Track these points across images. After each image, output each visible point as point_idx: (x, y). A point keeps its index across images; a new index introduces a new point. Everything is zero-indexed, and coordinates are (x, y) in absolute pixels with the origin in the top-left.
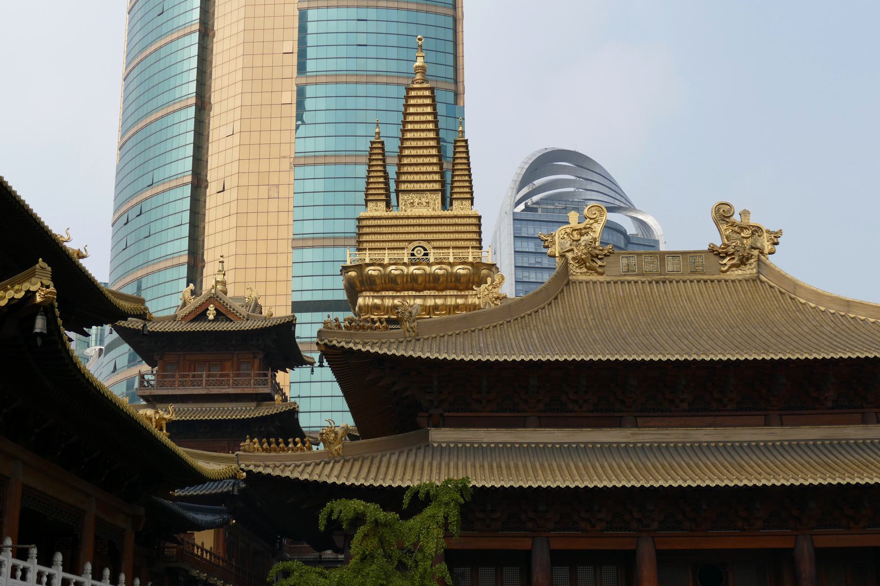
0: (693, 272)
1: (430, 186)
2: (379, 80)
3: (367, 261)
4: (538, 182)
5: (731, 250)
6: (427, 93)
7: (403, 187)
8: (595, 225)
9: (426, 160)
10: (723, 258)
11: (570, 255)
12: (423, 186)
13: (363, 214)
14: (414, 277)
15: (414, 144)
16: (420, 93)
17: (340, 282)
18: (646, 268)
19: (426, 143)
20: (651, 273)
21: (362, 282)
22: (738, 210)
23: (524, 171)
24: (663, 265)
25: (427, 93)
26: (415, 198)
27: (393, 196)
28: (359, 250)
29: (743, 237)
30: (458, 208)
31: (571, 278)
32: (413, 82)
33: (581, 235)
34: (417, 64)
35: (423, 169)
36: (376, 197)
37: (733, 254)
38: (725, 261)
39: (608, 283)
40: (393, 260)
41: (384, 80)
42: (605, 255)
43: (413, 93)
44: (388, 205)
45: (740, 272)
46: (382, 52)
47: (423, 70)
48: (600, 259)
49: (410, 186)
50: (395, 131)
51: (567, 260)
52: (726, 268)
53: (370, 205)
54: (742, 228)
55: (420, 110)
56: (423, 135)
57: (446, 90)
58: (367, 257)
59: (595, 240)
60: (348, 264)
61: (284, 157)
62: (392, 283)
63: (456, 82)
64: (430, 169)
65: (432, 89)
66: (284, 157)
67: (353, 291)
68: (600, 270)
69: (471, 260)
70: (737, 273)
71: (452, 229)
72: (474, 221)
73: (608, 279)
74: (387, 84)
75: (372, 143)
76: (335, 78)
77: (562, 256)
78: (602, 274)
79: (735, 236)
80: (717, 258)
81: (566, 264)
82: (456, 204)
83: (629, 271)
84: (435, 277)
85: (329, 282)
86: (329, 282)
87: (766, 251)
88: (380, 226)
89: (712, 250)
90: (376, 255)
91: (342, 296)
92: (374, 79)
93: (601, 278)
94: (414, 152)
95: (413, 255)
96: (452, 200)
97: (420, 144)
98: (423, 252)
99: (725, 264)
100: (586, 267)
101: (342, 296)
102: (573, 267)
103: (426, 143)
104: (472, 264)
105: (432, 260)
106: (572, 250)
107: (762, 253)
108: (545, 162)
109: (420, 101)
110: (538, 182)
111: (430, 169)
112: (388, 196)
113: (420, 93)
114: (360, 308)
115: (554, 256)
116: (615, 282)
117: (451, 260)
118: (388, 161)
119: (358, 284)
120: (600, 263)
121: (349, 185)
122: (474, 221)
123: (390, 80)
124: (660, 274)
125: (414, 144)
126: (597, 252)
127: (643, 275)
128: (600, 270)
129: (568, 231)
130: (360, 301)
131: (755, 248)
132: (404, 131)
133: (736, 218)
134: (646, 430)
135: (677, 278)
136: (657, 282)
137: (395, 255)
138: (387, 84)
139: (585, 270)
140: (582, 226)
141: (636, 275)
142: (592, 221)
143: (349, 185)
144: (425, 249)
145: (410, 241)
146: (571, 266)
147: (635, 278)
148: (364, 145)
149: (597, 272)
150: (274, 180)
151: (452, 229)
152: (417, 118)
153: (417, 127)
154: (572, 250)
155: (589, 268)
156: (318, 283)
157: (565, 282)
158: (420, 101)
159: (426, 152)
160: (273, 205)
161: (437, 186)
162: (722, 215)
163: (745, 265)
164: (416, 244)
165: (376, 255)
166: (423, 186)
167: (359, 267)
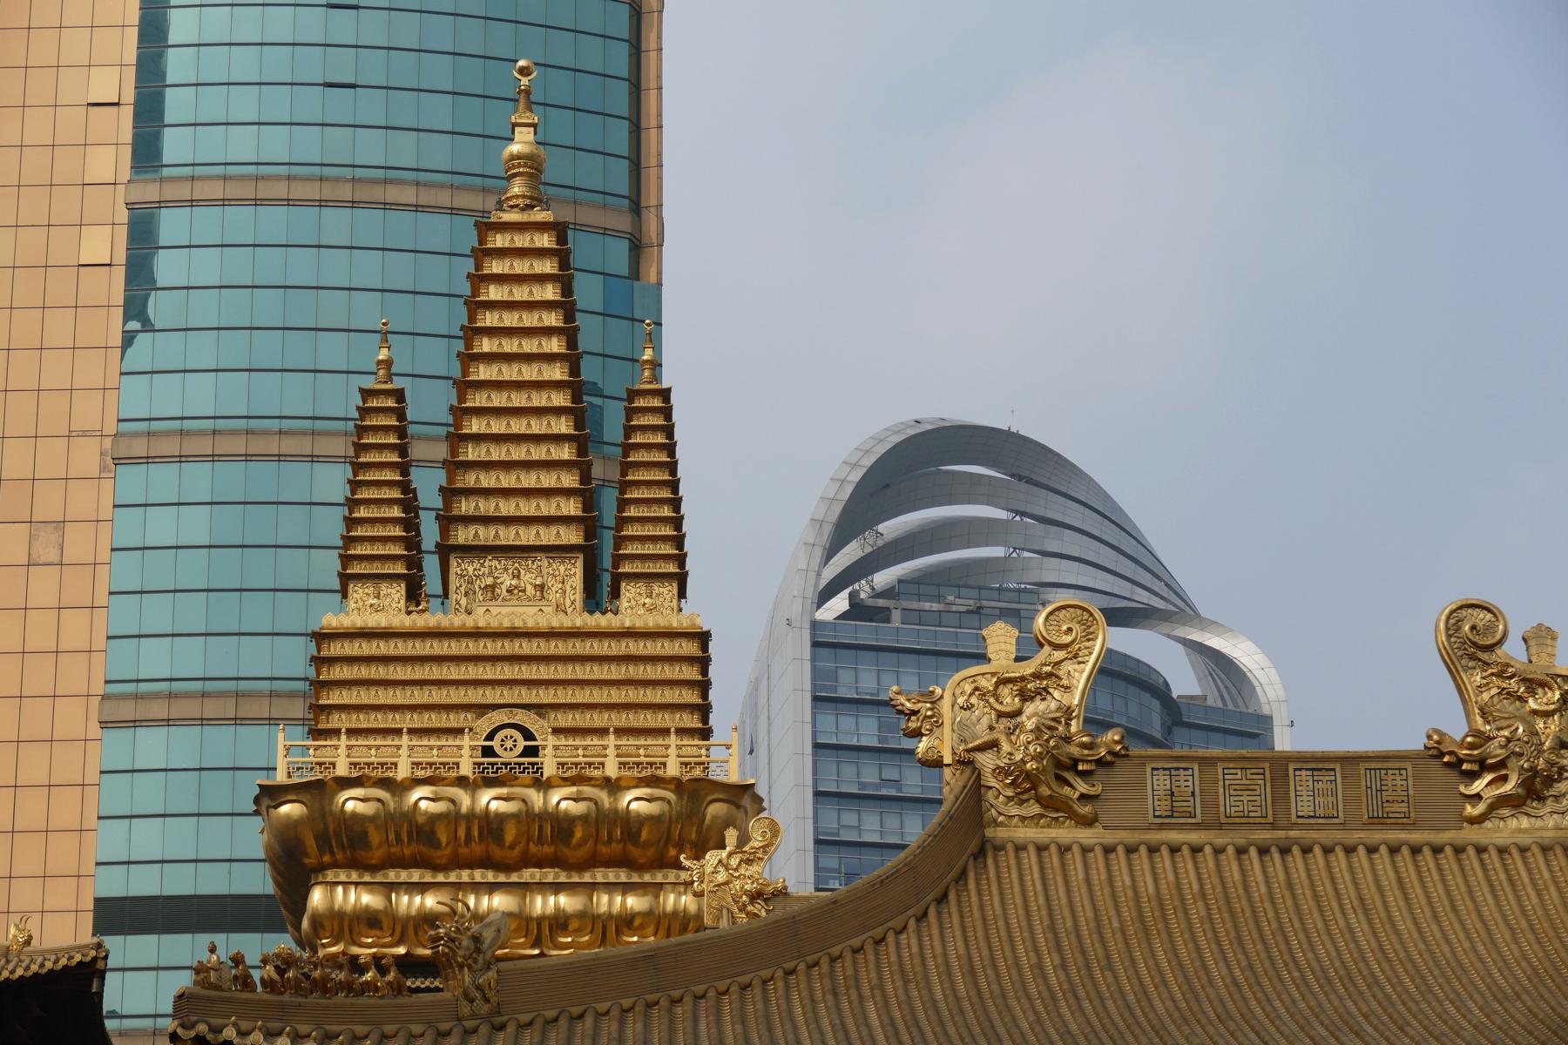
0: (1378, 821)
1: (548, 536)
2: (393, 194)
3: (342, 770)
4: (892, 527)
5: (1495, 751)
6: (545, 241)
7: (463, 535)
8: (1068, 666)
9: (538, 453)
10: (1473, 776)
11: (987, 761)
12: (527, 536)
13: (332, 620)
14: (491, 825)
15: (499, 399)
16: (522, 241)
17: (252, 838)
18: (1231, 805)
19: (539, 399)
21: (323, 840)
22: (1518, 623)
23: (849, 490)
24: (1281, 792)
25: (545, 241)
26: (503, 573)
27: (431, 564)
28: (316, 733)
29: (1535, 712)
30: (637, 606)
31: (989, 832)
32: (500, 207)
33: (1025, 697)
34: (515, 148)
35: (529, 480)
36: (377, 568)
37: (1502, 764)
38: (1478, 786)
39: (1108, 850)
40: (420, 767)
41: (409, 195)
42: (1100, 762)
43: (500, 241)
44: (414, 594)
45: (1525, 822)
46: (404, 109)
47: (533, 166)
49: (486, 535)
50: (439, 358)
51: (978, 775)
53: (358, 592)
55: (520, 293)
56: (529, 372)
57: (605, 232)
58: (341, 757)
59: (1068, 712)
60: (280, 777)
61: (84, 434)
62: (418, 845)
63: (636, 206)
64: (548, 480)
65: (560, 230)
66: (84, 434)
67: (294, 864)
68: (1085, 809)
69: (673, 770)
70: (1515, 827)
71: (616, 672)
72: (690, 648)
73: (1110, 838)
74: (417, 208)
75: (366, 393)
76: (252, 186)
77: (965, 762)
78: (1089, 822)
79: (1510, 707)
80: (1453, 776)
81: (976, 791)
82: (629, 591)
83: (1173, 816)
84: (561, 825)
85: (218, 838)
86: (218, 838)
88: (386, 660)
89: (1437, 751)
90: (371, 752)
91: (258, 881)
92: (377, 193)
93: (1086, 835)
94: (498, 426)
95: (488, 752)
96: (617, 579)
97: (519, 400)
98: (522, 743)
99: (1478, 797)
100: (1039, 799)
101: (258, 881)
102: (999, 797)
103: (539, 399)
104: (677, 785)
105: (549, 770)
106: (993, 745)
108: (917, 464)
109: (521, 267)
110: (892, 527)
111: (548, 480)
112: (414, 563)
113: (522, 241)
114: (317, 922)
115: (938, 764)
116: (1131, 850)
117: (612, 770)
118: (417, 451)
119: (311, 844)
120: (1082, 787)
121: (292, 525)
122: (690, 648)
123: (426, 197)
124: (1274, 826)
125: (499, 399)
126: (1075, 751)
127: (1220, 826)
128: (1085, 809)
129: (987, 684)
130: (317, 897)
132: (469, 358)
133: (1513, 650)
135: (1328, 837)
136: (1263, 851)
137: (432, 751)
138: (417, 208)
139: (1035, 809)
140: (1027, 669)
142: (1059, 655)
143: (292, 525)
144: (528, 735)
145: (482, 709)
146: (990, 795)
147: (1194, 837)
148: (342, 400)
149: (1073, 816)
150: (48, 505)
151: (616, 672)
152: (510, 319)
153: (510, 346)
154: (993, 745)
155: (1052, 805)
156: (180, 838)
157: (973, 846)
158: (521, 267)
159: (537, 426)
160: (44, 586)
161: (572, 536)
162: (1470, 642)
163: (1541, 799)
164: (499, 717)
165: (371, 752)
166: (527, 536)
167: (317, 790)
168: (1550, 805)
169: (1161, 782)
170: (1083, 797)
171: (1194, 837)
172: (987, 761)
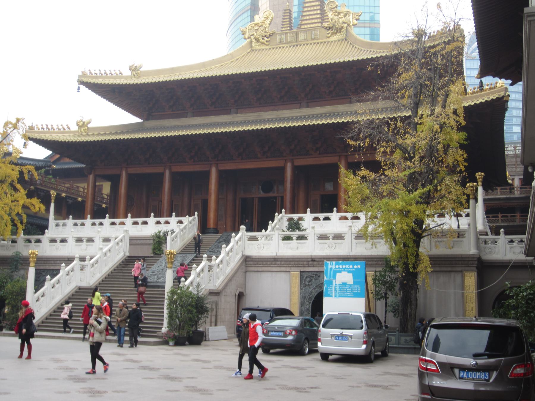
0: (312, 39)
10: (328, 30)
11: (252, 37)
18: (290, 39)
20: (292, 42)
24: (298, 37)
37: (332, 27)
48: (267, 38)
52: (330, 35)
54: (339, 13)
79: (336, 17)
87: (351, 24)
93: (267, 47)
107: (349, 25)
127: (288, 43)
131: (345, 23)
134: (239, 115)
141: (285, 43)
154: (253, 35)
163: (340, 32)
168: (342, 33)
169: (279, 37)
170: (267, 41)
171: (283, 45)
172: (252, 37)
